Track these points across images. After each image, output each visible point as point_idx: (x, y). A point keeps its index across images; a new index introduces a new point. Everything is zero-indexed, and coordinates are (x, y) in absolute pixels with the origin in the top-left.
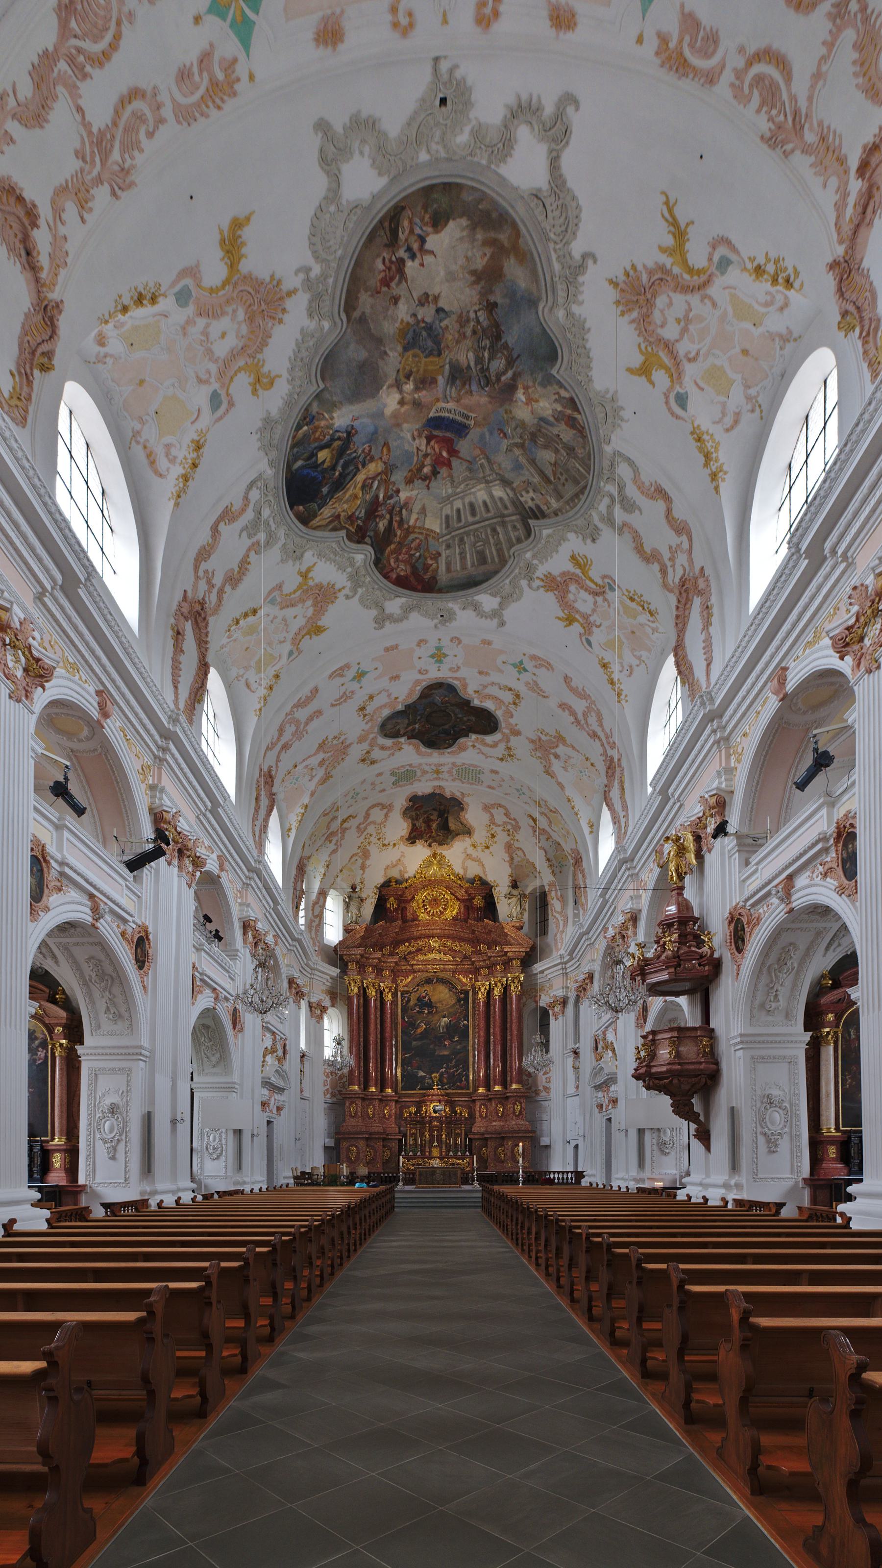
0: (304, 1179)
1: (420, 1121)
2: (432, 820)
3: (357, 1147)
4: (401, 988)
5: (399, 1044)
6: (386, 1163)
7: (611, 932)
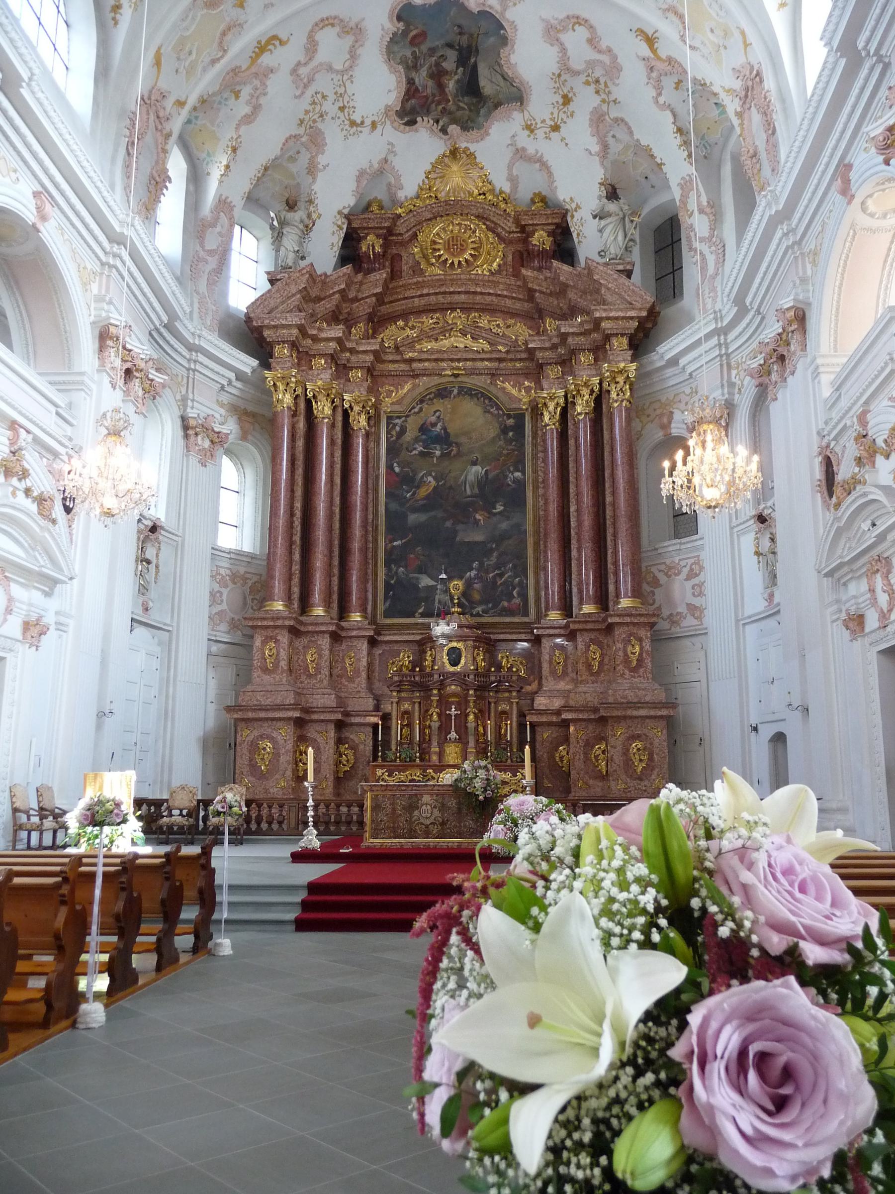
2: (445, 72)
4: (388, 405)
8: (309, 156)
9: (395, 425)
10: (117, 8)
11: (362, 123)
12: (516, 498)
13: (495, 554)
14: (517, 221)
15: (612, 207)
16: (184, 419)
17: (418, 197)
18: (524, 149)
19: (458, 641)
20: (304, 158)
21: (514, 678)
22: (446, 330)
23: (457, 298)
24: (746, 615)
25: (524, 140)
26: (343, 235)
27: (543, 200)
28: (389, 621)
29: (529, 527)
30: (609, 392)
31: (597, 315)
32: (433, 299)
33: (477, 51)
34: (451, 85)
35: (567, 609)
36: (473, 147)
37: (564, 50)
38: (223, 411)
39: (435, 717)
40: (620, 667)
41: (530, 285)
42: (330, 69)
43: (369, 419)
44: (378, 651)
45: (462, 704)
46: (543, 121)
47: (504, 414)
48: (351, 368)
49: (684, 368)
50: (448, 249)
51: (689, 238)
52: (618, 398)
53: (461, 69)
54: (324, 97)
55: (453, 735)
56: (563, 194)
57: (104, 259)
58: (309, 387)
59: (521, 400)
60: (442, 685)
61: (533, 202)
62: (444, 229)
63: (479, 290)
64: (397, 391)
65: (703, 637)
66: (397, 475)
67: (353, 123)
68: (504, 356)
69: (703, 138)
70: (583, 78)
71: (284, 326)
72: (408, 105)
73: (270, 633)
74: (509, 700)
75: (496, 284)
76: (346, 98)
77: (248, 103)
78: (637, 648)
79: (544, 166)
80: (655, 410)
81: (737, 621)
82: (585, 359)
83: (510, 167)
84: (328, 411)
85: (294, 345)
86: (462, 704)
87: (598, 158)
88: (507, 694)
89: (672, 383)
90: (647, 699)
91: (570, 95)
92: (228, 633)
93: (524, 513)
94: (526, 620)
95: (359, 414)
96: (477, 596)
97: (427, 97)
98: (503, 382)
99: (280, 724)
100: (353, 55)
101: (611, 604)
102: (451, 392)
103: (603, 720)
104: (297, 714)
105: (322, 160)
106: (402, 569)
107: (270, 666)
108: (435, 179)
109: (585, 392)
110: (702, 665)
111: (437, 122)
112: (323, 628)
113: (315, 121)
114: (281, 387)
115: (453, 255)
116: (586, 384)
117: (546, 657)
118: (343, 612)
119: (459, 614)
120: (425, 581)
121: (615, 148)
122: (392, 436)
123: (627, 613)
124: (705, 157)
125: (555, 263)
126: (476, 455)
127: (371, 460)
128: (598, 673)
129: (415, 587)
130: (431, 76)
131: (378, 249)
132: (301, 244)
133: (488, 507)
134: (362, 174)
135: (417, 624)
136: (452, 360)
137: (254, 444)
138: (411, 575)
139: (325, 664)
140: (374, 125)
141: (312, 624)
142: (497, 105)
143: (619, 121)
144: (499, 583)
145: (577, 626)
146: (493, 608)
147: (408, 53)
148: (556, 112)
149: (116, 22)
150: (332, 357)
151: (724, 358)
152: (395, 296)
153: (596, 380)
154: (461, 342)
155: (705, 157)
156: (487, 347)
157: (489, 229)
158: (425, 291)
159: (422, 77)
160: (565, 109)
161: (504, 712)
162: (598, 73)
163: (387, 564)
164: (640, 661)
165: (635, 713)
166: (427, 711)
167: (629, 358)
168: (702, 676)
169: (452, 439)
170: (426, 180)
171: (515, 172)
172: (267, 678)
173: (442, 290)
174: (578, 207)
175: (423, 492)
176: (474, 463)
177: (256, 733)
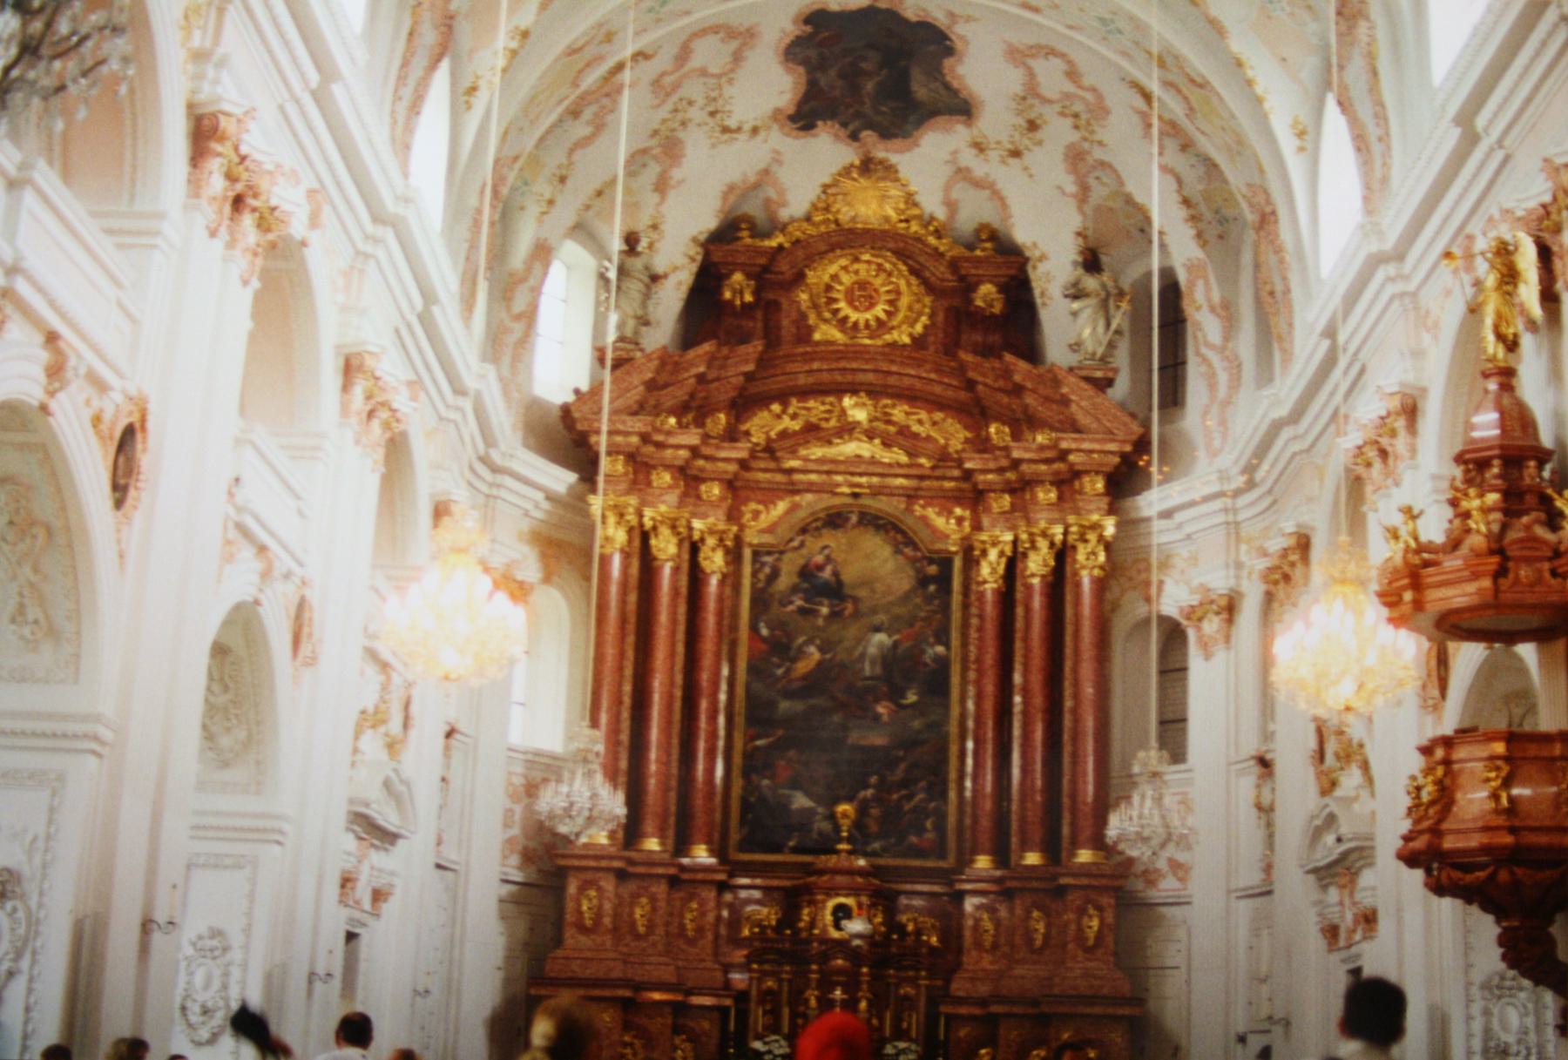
5: (740, 705)
9: (763, 564)
10: (473, 89)
11: (739, 129)
12: (937, 684)
13: (902, 766)
15: (1091, 283)
17: (808, 219)
18: (968, 170)
19: (847, 896)
20: (653, 170)
21: (924, 950)
22: (847, 430)
23: (861, 377)
25: (968, 158)
26: (694, 268)
29: (953, 729)
30: (1074, 548)
31: (1064, 445)
32: (825, 377)
35: (1002, 856)
36: (894, 158)
37: (1031, 75)
39: (813, 1002)
40: (1071, 946)
41: (971, 374)
42: (703, 72)
43: (727, 551)
46: (998, 143)
47: (924, 558)
48: (704, 480)
49: (1180, 526)
50: (851, 303)
51: (1195, 337)
52: (1088, 563)
53: (884, 72)
54: (690, 103)
56: (1022, 235)
57: (444, 412)
58: (648, 513)
59: (947, 537)
60: (825, 958)
61: (978, 231)
62: (845, 268)
63: (894, 368)
64: (768, 513)
65: (1186, 907)
66: (764, 640)
67: (726, 130)
68: (927, 472)
70: (1057, 108)
72: (807, 108)
73: (589, 876)
74: (913, 981)
75: (919, 363)
76: (721, 102)
77: (588, 123)
78: (1095, 923)
79: (997, 196)
80: (1139, 572)
81: (1229, 892)
82: (1045, 495)
83: (947, 188)
84: (672, 549)
86: (851, 986)
87: (1072, 205)
88: (911, 973)
89: (1164, 539)
90: (1105, 991)
91: (1039, 122)
92: (520, 868)
93: (946, 707)
94: (942, 864)
95: (713, 550)
98: (923, 507)
100: (737, 58)
101: (1064, 854)
102: (847, 519)
104: (627, 993)
105: (677, 174)
106: (766, 782)
107: (588, 923)
108: (834, 195)
109: (1043, 544)
112: (660, 871)
113: (673, 130)
115: (856, 309)
116: (1044, 534)
118: (682, 845)
119: (850, 853)
120: (801, 801)
121: (1099, 193)
122: (759, 580)
123: (1085, 871)
124: (1221, 237)
126: (881, 618)
127: (727, 613)
128: (1043, 948)
129: (784, 807)
130: (842, 76)
131: (748, 298)
132: (644, 305)
133: (895, 694)
134: (731, 188)
135: (785, 864)
136: (852, 474)
137: (561, 589)
138: (781, 791)
140: (755, 131)
141: (644, 864)
144: (907, 808)
145: (1014, 884)
147: (813, 53)
148: (1017, 136)
149: (469, 106)
151: (1232, 526)
152: (772, 371)
153: (1058, 530)
155: (1221, 237)
156: (904, 459)
157: (913, 271)
158: (816, 365)
160: (1030, 135)
161: (906, 998)
162: (1078, 107)
163: (746, 774)
164: (1099, 937)
165: (1088, 1010)
166: (802, 992)
167: (1106, 507)
169: (848, 591)
170: (823, 197)
171: (955, 195)
172: (584, 940)
174: (1042, 258)
175: (802, 667)
176: (877, 629)
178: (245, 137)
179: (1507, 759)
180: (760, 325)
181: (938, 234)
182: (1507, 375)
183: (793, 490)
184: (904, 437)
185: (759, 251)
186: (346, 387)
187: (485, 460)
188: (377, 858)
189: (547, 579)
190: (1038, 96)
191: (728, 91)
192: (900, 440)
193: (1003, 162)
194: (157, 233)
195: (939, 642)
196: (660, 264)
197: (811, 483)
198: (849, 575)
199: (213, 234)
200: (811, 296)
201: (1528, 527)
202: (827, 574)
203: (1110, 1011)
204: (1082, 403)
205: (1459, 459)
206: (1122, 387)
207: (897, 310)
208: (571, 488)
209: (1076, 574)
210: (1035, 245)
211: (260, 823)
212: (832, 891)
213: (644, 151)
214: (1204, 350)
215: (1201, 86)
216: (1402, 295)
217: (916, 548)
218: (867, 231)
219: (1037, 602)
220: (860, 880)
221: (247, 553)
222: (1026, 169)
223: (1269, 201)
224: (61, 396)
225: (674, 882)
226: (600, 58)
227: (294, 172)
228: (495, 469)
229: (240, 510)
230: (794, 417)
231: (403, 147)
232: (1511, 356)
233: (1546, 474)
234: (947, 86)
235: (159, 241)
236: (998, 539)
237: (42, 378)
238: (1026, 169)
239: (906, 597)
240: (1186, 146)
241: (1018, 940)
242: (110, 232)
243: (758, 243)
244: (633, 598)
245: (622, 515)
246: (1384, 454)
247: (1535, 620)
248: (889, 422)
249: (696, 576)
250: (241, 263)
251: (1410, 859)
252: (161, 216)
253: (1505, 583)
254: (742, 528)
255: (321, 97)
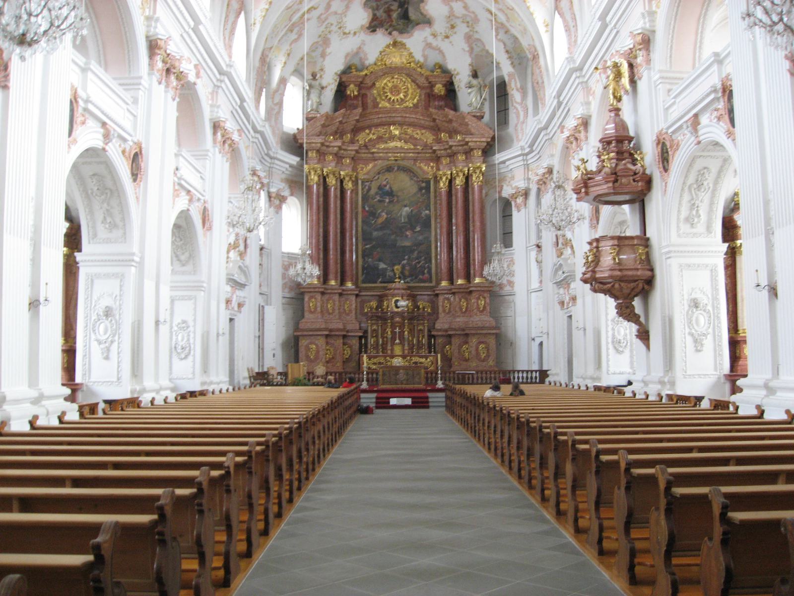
0: (262, 378)
1: (381, 317)
2: (392, 10)
3: (316, 345)
6: (346, 362)
7: (567, 133)
8: (321, 49)
11: (349, 33)
12: (427, 224)
13: (416, 252)
14: (427, 78)
15: (475, 82)
16: (269, 193)
17: (375, 64)
18: (430, 44)
20: (320, 50)
22: (392, 138)
23: (396, 119)
24: (532, 287)
25: (431, 39)
26: (337, 84)
27: (440, 67)
28: (365, 285)
29: (433, 239)
30: (472, 175)
31: (467, 140)
32: (384, 120)
33: (408, 3)
34: (395, 15)
35: (451, 280)
36: (404, 41)
37: (451, 8)
38: (284, 185)
39: (389, 333)
40: (475, 311)
41: (434, 116)
42: (336, 13)
43: (353, 182)
44: (359, 300)
45: (402, 326)
48: (344, 158)
50: (391, 93)
51: (512, 100)
52: (476, 181)
53: (400, 10)
54: (332, 24)
55: (397, 341)
56: (451, 66)
58: (325, 170)
60: (392, 318)
61: (435, 66)
63: (407, 115)
66: (367, 211)
67: (345, 33)
69: (518, 54)
70: (461, 20)
71: (313, 143)
72: (373, 24)
73: (311, 294)
75: (416, 113)
78: (483, 302)
79: (441, 52)
81: (528, 291)
82: (461, 157)
83: (424, 50)
84: (334, 182)
85: (318, 151)
87: (468, 54)
89: (502, 171)
90: (487, 325)
92: (289, 292)
93: (430, 232)
96: (407, 273)
97: (382, 21)
99: (319, 337)
103: (467, 335)
104: (327, 333)
105: (328, 51)
106: (370, 260)
107: (313, 310)
109: (461, 174)
110: (513, 308)
111: (387, 30)
114: (313, 173)
115: (393, 95)
116: (461, 171)
117: (440, 304)
118: (343, 282)
120: (382, 266)
123: (478, 286)
124: (520, 64)
125: (446, 110)
129: (376, 268)
130: (385, 12)
131: (356, 93)
132: (319, 97)
133: (412, 228)
137: (296, 197)
139: (336, 308)
140: (355, 33)
142: (418, 24)
143: (479, 40)
146: (416, 278)
148: (447, 31)
150: (336, 154)
153: (466, 169)
154: (399, 144)
156: (412, 147)
158: (380, 116)
159: (381, 13)
161: (421, 330)
162: (468, 19)
163: (364, 257)
164: (484, 307)
168: (513, 315)
169: (394, 193)
171: (426, 53)
172: (311, 316)
173: (389, 115)
174: (458, 74)
175: (380, 220)
176: (405, 206)
177: (308, 341)
178: (168, 47)
179: (618, 246)
180: (360, 102)
181: (421, 67)
182: (617, 110)
183: (375, 160)
184: (411, 139)
185: (358, 77)
186: (215, 133)
187: (267, 155)
188: (239, 293)
189: (292, 195)
190: (454, 15)
191: (345, 20)
192: (411, 140)
193: (443, 40)
194: (140, 84)
195: (426, 209)
196: (324, 83)
197: (380, 157)
198: (394, 189)
199: (160, 83)
200: (378, 92)
201: (625, 164)
202: (387, 187)
203: (489, 331)
204: (473, 123)
205: (601, 141)
206: (487, 118)
207: (408, 95)
208: (298, 163)
209: (472, 184)
210: (455, 70)
211: (196, 284)
212: (394, 295)
213: (317, 42)
214: (515, 104)
215: (511, 10)
216: (582, 83)
217: (418, 178)
218: (396, 68)
219: (460, 195)
220: (403, 291)
221: (183, 193)
222: (451, 42)
223: (536, 50)
224: (110, 144)
225: (341, 295)
226: (299, 10)
227: (189, 58)
228: (271, 158)
229: (179, 179)
230: (374, 134)
231: (229, 47)
232: (619, 104)
233: (632, 145)
234: (422, 14)
235: (141, 87)
236: (445, 172)
237: (101, 138)
238: (451, 42)
239: (415, 194)
240: (507, 32)
241: (457, 309)
242: (120, 85)
243: (358, 73)
244: (321, 199)
245: (316, 171)
246: (576, 139)
247: (627, 197)
248: (406, 134)
249: (343, 191)
250: (171, 93)
251: (585, 281)
252: (141, 78)
253: (617, 185)
254: (357, 173)
255: (196, 30)
